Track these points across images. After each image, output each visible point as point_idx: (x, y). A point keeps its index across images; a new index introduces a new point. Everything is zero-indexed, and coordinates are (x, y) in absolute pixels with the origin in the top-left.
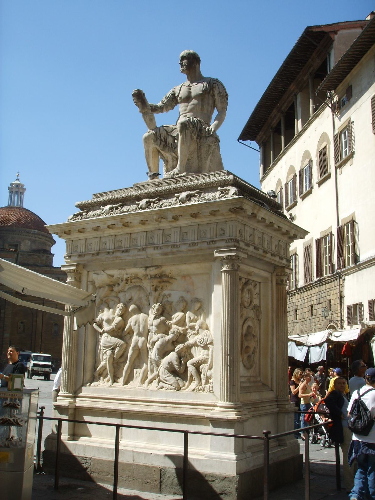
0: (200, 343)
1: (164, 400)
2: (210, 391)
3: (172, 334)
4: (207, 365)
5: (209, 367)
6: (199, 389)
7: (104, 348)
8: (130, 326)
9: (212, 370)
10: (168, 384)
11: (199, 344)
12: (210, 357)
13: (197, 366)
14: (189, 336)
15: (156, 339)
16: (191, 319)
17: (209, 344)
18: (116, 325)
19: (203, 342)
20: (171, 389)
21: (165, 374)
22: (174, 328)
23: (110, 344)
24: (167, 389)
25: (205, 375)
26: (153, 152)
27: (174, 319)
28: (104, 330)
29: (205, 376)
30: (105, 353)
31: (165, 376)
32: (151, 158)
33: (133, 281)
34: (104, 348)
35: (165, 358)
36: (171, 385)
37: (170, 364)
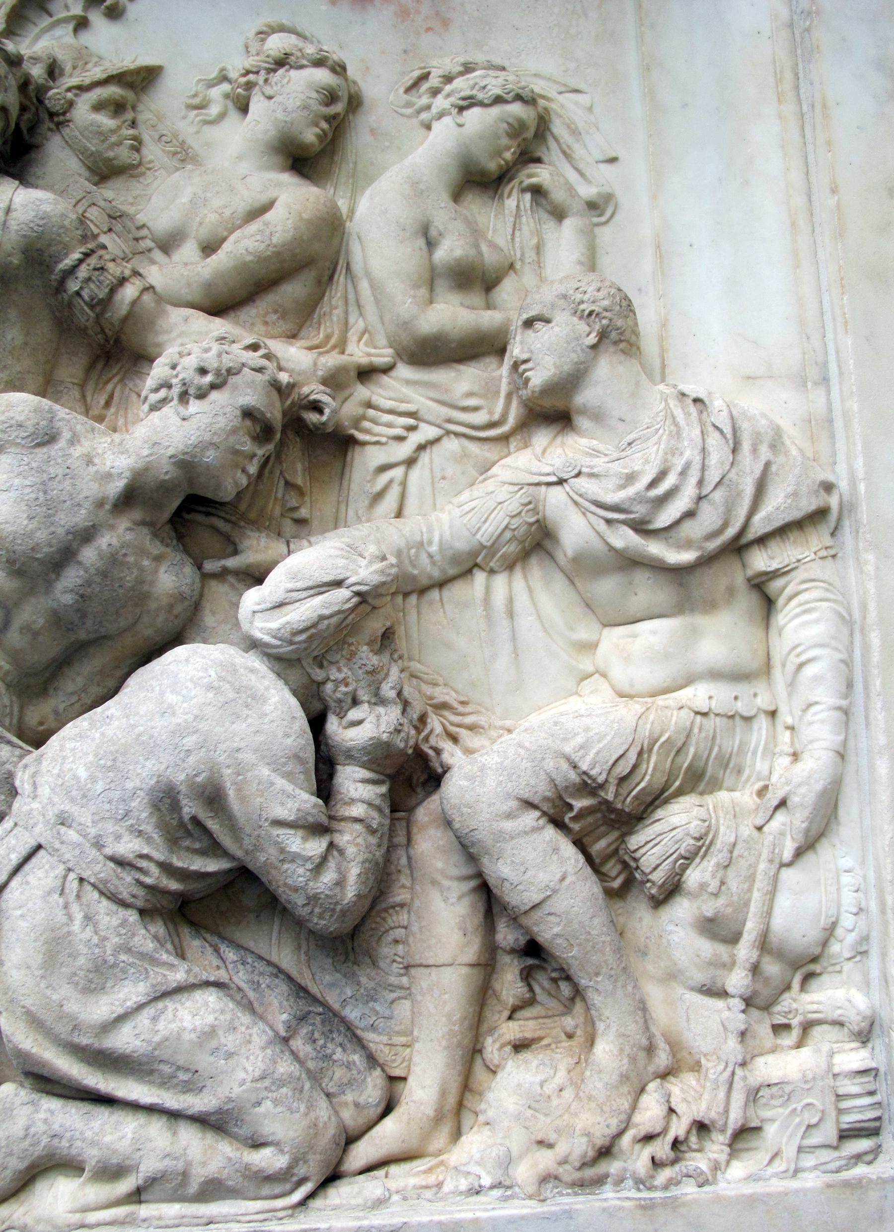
0: (641, 527)
2: (845, 1135)
3: (201, 395)
4: (745, 797)
5: (807, 831)
6: (678, 1128)
9: (839, 857)
11: (576, 531)
12: (819, 688)
14: (404, 450)
16: (442, 254)
17: (783, 531)
19: (690, 514)
20: (214, 1189)
21: (100, 976)
22: (189, 342)
25: (751, 929)
27: (188, 251)
29: (745, 951)
31: (101, 1009)
36: (213, 1123)
37: (192, 812)
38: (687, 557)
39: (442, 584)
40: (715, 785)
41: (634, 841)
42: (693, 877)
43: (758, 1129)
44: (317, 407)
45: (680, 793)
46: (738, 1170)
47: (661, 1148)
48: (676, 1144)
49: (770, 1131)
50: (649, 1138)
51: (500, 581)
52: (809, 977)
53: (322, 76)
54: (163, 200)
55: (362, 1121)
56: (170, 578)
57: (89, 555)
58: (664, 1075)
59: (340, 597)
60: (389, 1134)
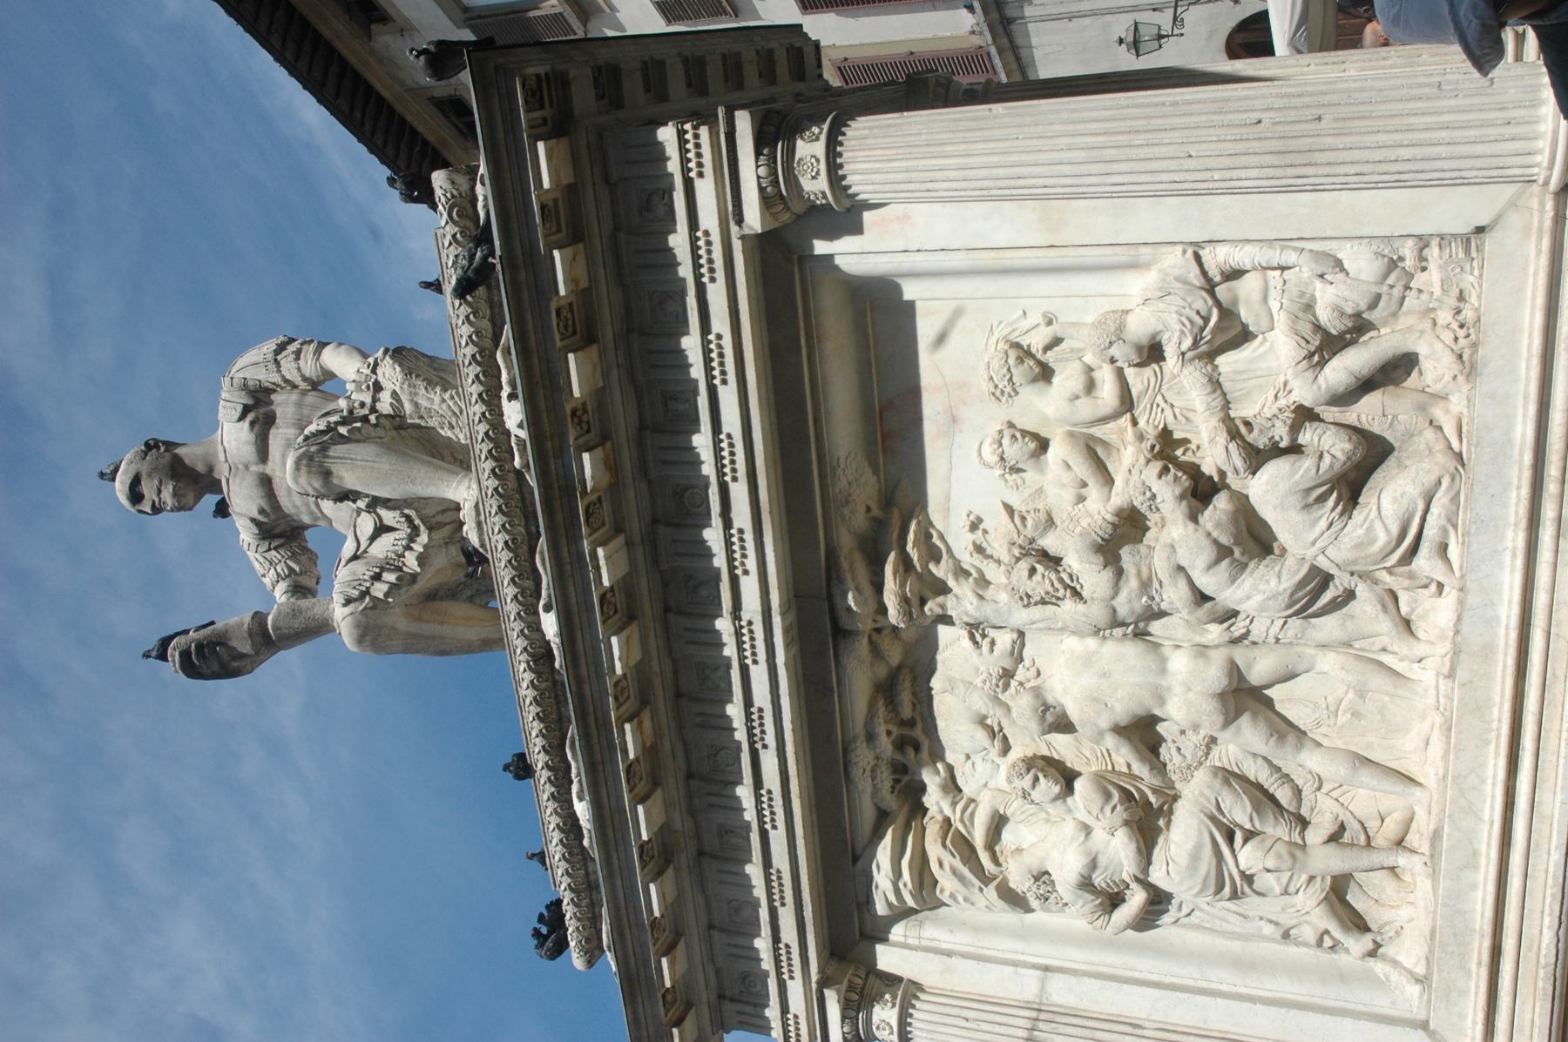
1: (1516, 539)
6: (1455, 326)
7: (1227, 890)
8: (1118, 730)
10: (1423, 520)
13: (1327, 345)
14: (1168, 412)
15: (1182, 584)
18: (1108, 809)
20: (1455, 500)
23: (1208, 851)
24: (1455, 526)
26: (420, 619)
28: (1138, 880)
30: (1249, 879)
32: (446, 630)
33: (907, 712)
34: (1227, 890)
35: (1283, 535)
37: (1312, 498)
38: (1215, 312)
39: (1224, 394)
40: (1313, 299)
41: (1334, 332)
42: (1350, 311)
43: (1461, 292)
44: (1153, 447)
45: (1314, 315)
46: (1474, 300)
47: (1461, 333)
48: (1461, 326)
49: (1462, 286)
50: (1456, 339)
51: (1221, 369)
52: (1401, 259)
53: (1006, 441)
54: (1059, 497)
55: (1442, 441)
56: (1221, 502)
57: (1215, 534)
58: (1435, 323)
59: (1232, 446)
60: (1450, 430)
